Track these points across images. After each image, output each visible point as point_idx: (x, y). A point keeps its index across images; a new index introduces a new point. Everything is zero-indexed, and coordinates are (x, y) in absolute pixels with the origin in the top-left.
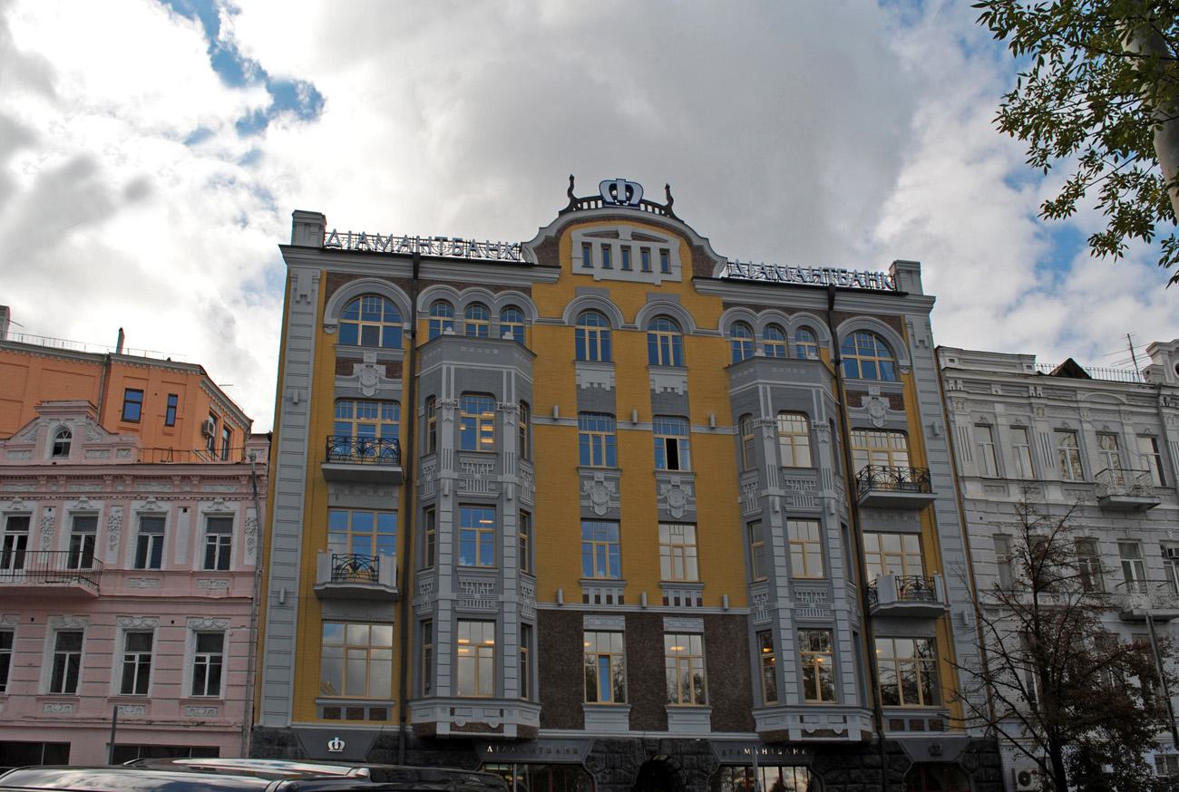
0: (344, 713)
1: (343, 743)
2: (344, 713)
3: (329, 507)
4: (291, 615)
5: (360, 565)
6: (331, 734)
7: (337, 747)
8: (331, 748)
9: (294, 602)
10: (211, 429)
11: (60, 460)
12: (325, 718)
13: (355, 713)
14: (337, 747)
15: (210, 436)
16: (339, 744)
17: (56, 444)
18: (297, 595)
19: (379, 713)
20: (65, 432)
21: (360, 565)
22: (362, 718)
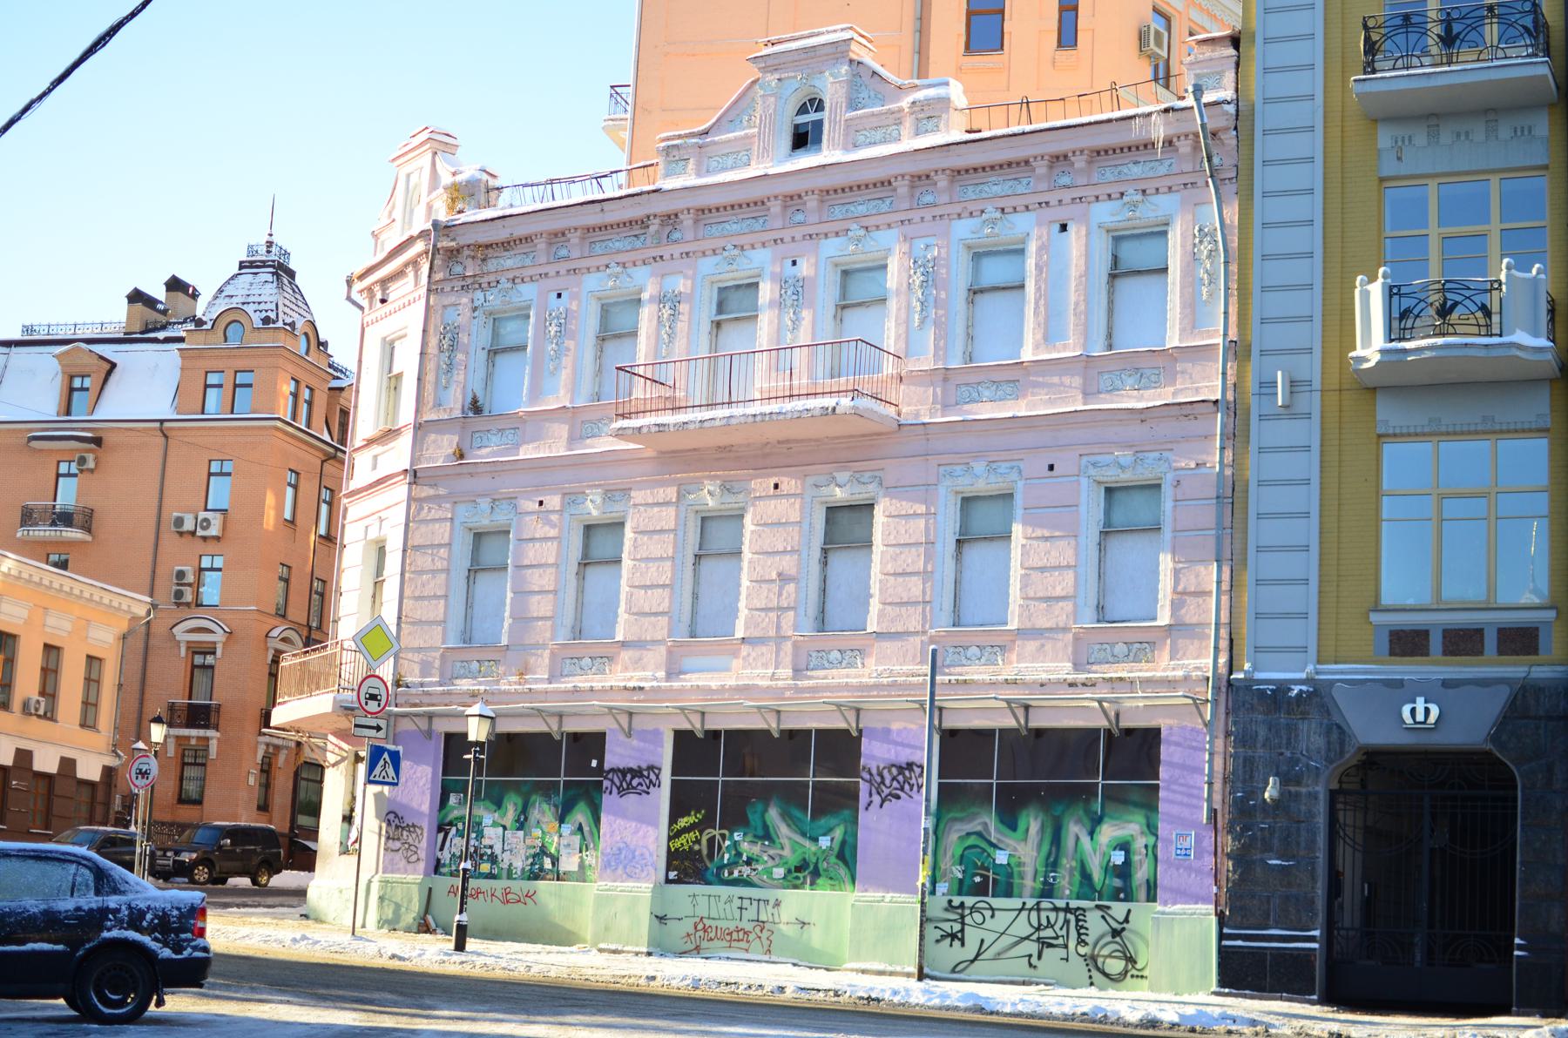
0: (1436, 642)
1: (1435, 711)
2: (1436, 642)
3: (1382, 180)
4: (1307, 432)
5: (1456, 304)
6: (1400, 690)
7: (1420, 717)
8: (1409, 720)
9: (1311, 402)
10: (1159, 43)
11: (806, 160)
12: (1392, 653)
13: (1463, 641)
14: (1420, 717)
15: (1158, 57)
16: (1427, 711)
17: (797, 127)
18: (1317, 384)
19: (1519, 640)
20: (812, 101)
21: (1456, 304)
22: (1479, 652)
